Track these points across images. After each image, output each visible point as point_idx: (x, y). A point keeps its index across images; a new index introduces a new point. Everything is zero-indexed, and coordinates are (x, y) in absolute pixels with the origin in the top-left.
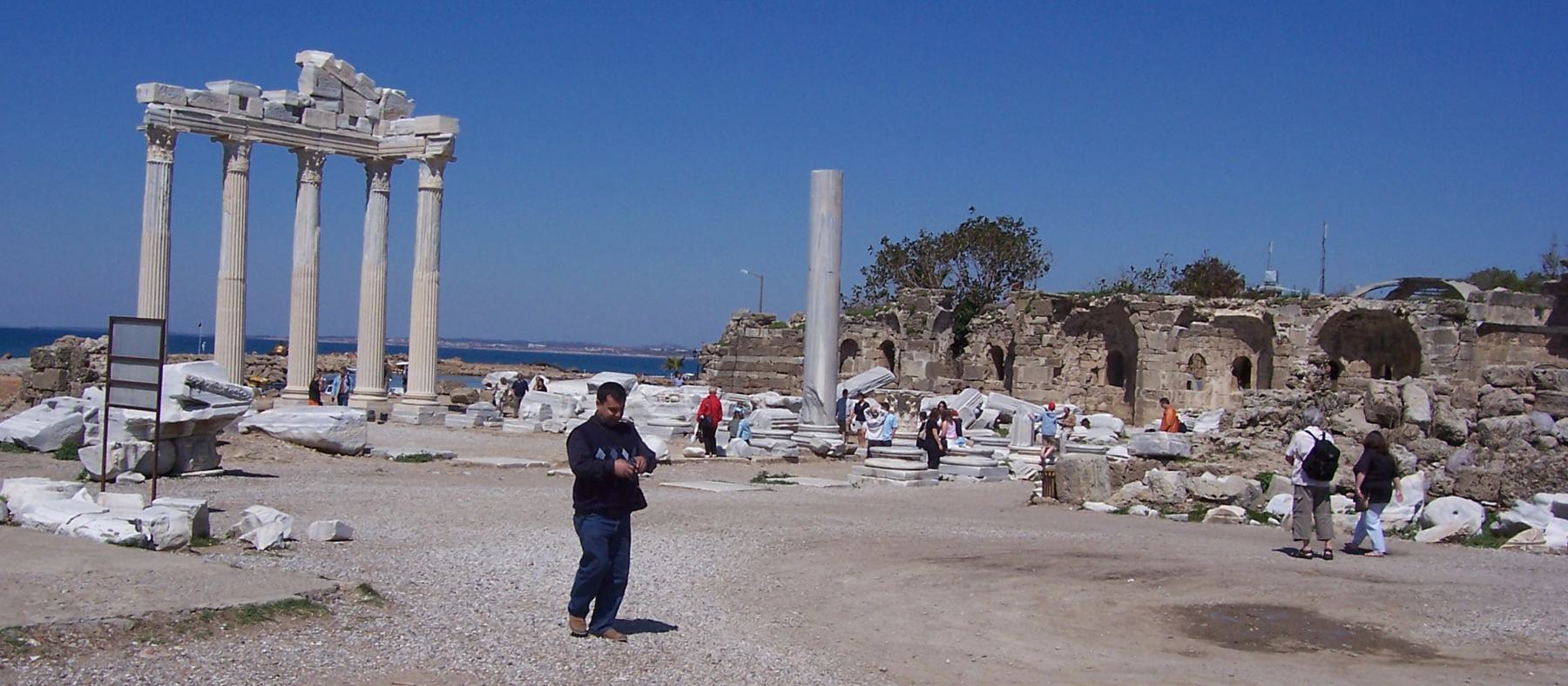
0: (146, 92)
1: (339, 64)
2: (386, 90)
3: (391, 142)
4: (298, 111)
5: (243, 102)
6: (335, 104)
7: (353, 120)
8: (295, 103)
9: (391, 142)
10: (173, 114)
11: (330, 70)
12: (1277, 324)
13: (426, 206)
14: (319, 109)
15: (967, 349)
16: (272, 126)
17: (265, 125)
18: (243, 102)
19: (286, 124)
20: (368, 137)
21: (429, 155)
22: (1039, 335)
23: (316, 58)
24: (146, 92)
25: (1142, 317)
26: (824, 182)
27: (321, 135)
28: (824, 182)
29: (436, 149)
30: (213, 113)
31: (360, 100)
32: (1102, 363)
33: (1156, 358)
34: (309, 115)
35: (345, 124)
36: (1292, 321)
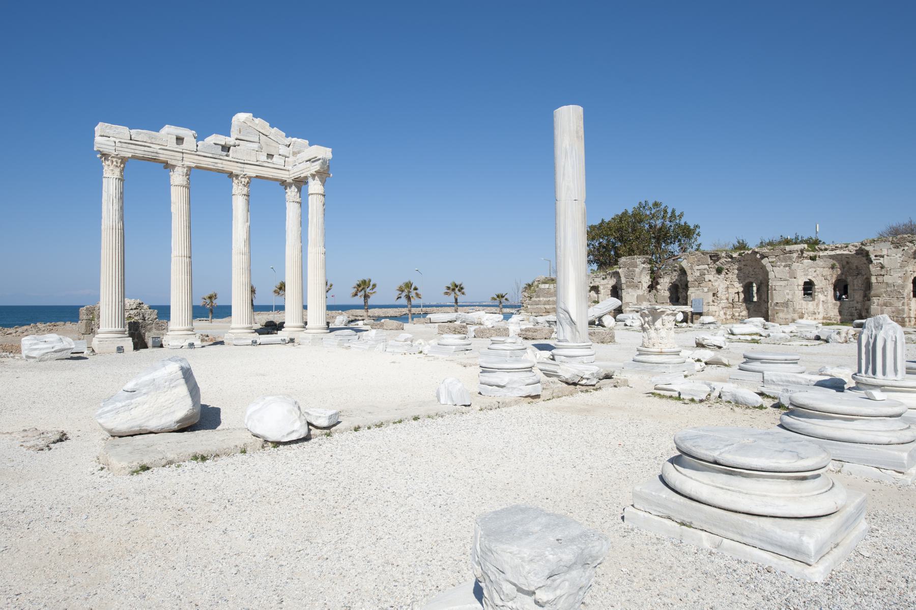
0: (100, 128)
1: (258, 121)
2: (294, 139)
3: (295, 169)
4: (226, 148)
6: (255, 146)
7: (270, 156)
8: (223, 143)
9: (295, 169)
10: (119, 145)
11: (249, 124)
12: (873, 257)
13: (315, 204)
15: (659, 287)
18: (180, 140)
20: (282, 167)
21: (313, 172)
22: (702, 274)
23: (241, 118)
24: (100, 128)
25: (771, 260)
26: (569, 120)
28: (569, 120)
29: (316, 167)
31: (275, 144)
32: (741, 289)
33: (783, 283)
35: (263, 158)
36: (885, 252)
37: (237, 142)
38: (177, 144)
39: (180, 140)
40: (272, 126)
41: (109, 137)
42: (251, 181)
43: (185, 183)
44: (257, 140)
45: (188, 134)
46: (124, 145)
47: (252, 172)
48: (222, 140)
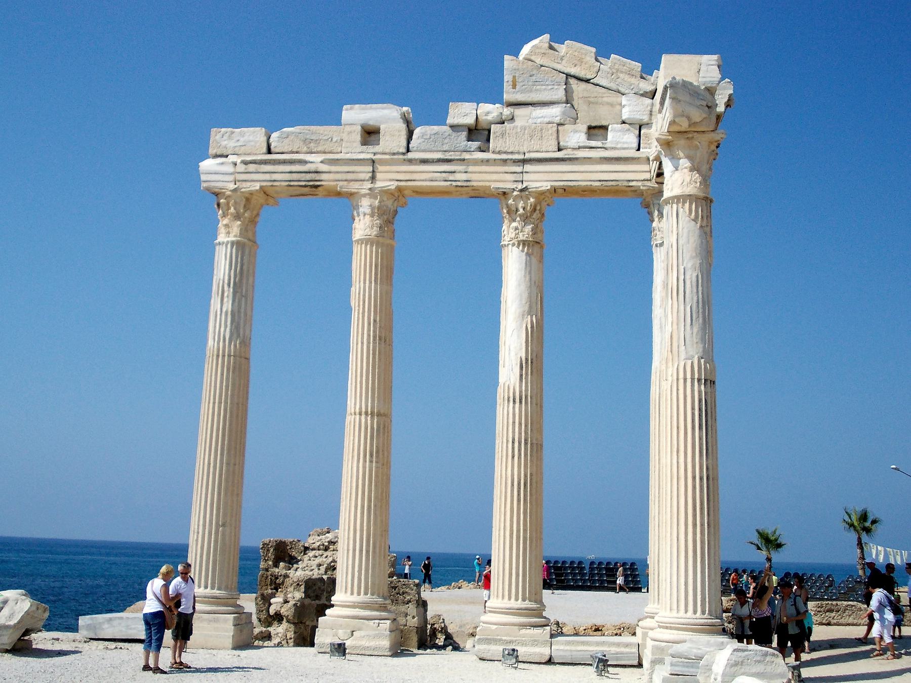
4: (478, 133)
5: (370, 134)
6: (555, 112)
7: (597, 130)
8: (470, 120)
10: (241, 168)
11: (539, 61)
14: (519, 123)
16: (424, 161)
17: (410, 161)
19: (448, 156)
20: (633, 153)
27: (524, 162)
30: (308, 157)
34: (503, 135)
35: (576, 137)
37: (507, 111)
38: (364, 143)
39: (370, 134)
40: (602, 53)
41: (231, 157)
42: (542, 208)
43: (375, 231)
44: (560, 94)
45: (388, 116)
46: (252, 167)
47: (540, 179)
48: (463, 113)
